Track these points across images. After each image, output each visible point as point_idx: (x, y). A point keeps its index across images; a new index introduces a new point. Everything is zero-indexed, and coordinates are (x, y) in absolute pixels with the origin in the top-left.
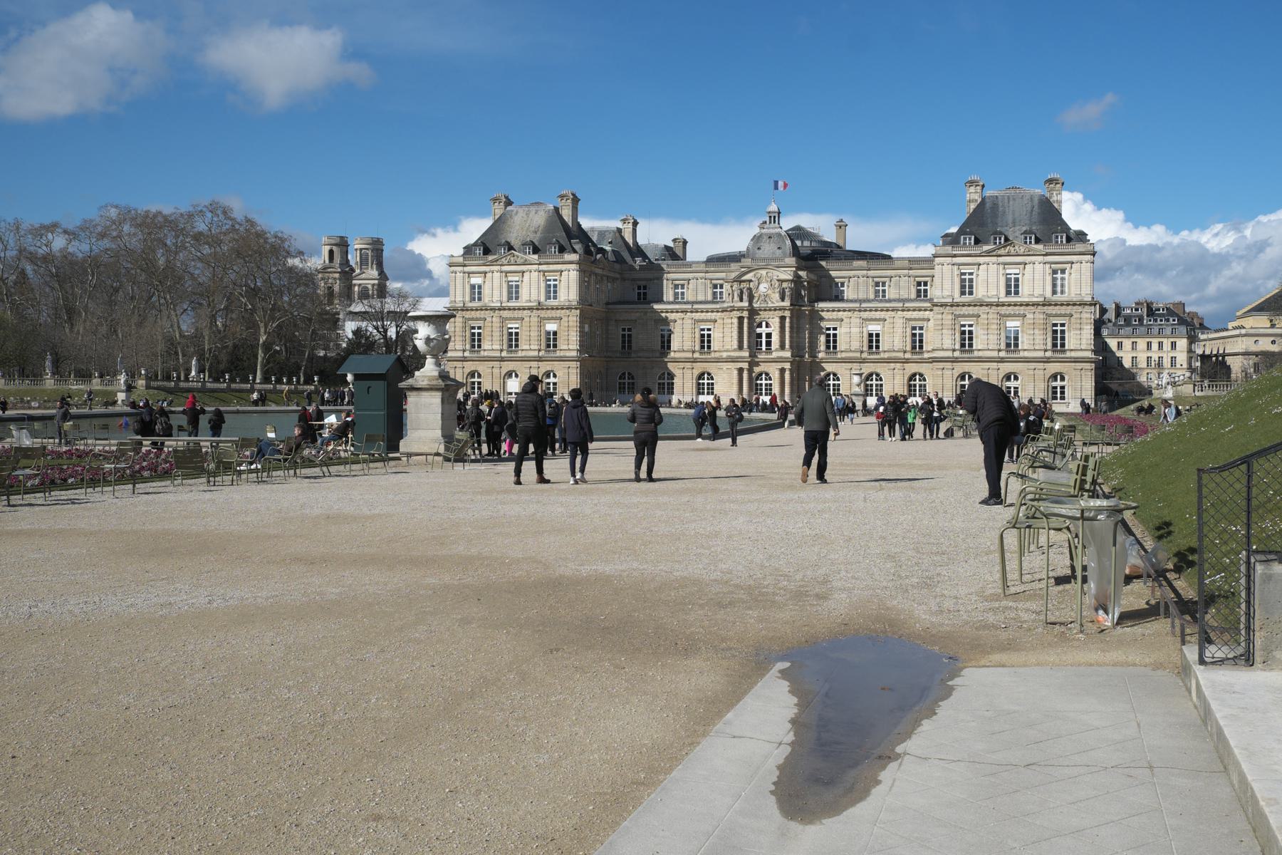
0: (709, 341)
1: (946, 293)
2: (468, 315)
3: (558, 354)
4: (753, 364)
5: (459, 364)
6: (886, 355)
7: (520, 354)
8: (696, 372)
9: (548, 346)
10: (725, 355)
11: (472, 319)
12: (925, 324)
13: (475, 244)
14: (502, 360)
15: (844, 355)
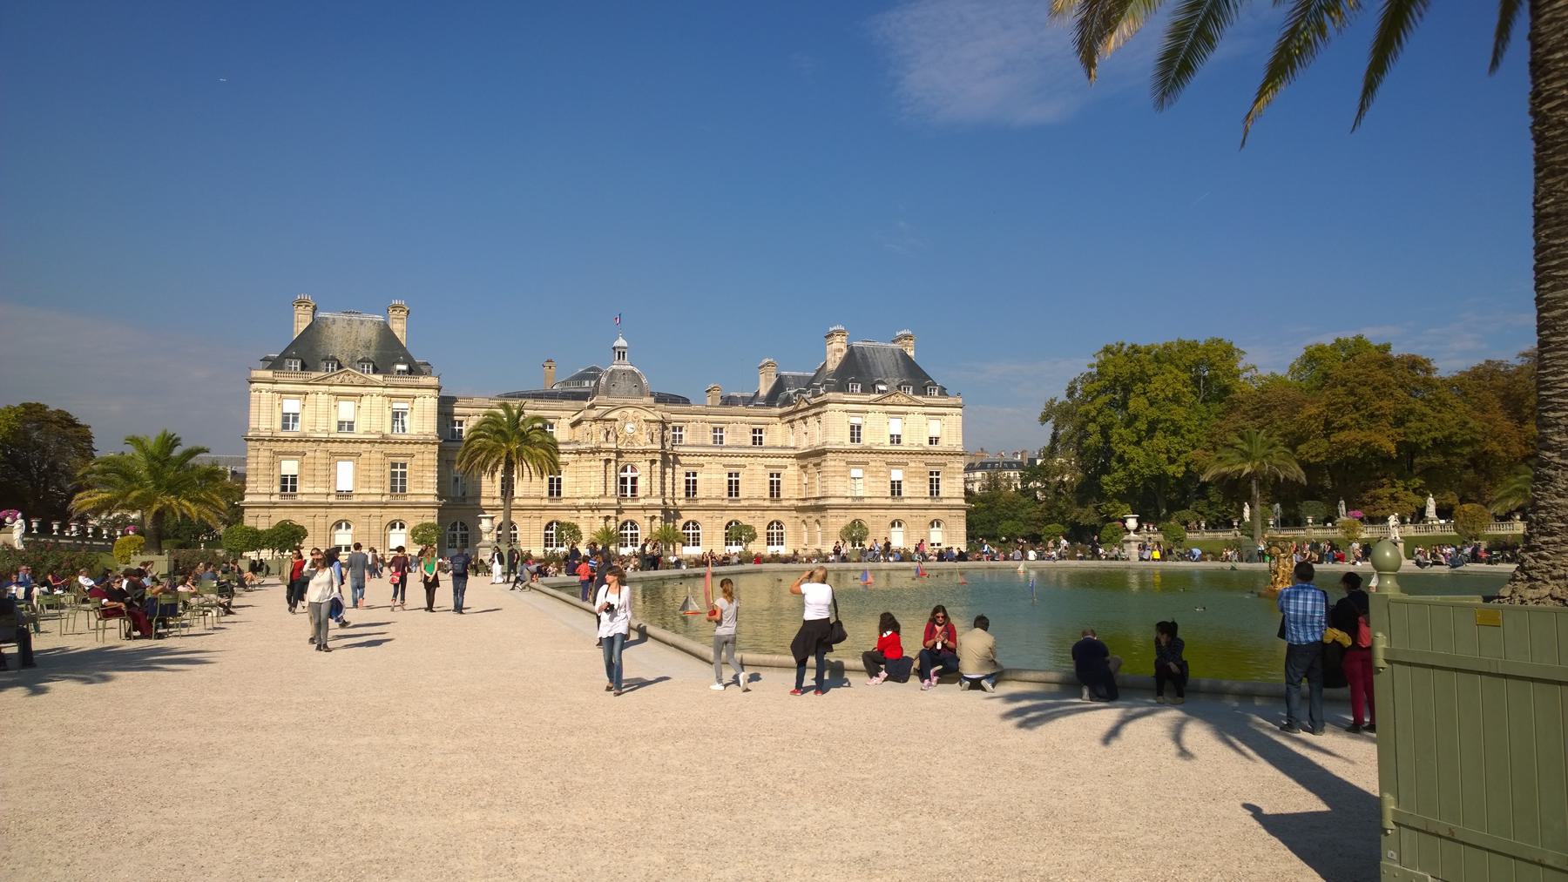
0: (559, 487)
1: (837, 440)
2: (278, 447)
3: (409, 499)
4: (620, 511)
5: (264, 512)
6: (745, 503)
7: (355, 499)
8: (545, 522)
9: (393, 489)
10: (582, 502)
11: (284, 453)
12: (783, 471)
13: (285, 355)
14: (330, 506)
15: (705, 503)
